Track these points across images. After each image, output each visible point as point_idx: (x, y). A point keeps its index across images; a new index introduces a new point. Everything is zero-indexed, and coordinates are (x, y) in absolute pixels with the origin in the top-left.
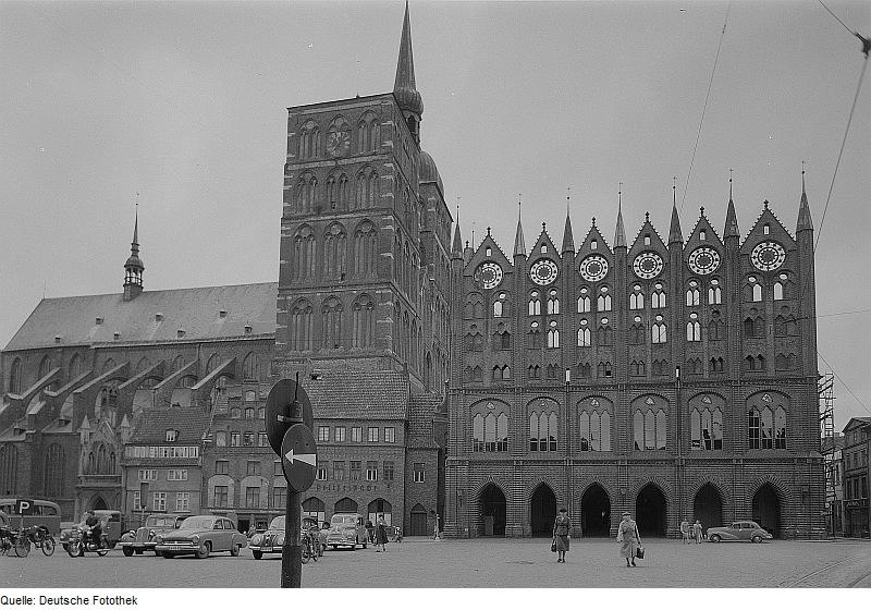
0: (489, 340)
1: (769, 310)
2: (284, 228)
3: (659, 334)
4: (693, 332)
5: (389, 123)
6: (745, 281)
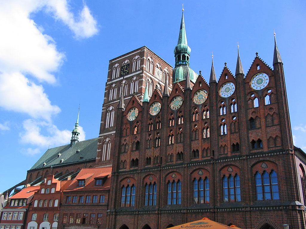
0: (130, 146)
1: (262, 111)
2: (103, 108)
3: (207, 134)
4: (224, 130)
5: (143, 58)
6: (248, 97)
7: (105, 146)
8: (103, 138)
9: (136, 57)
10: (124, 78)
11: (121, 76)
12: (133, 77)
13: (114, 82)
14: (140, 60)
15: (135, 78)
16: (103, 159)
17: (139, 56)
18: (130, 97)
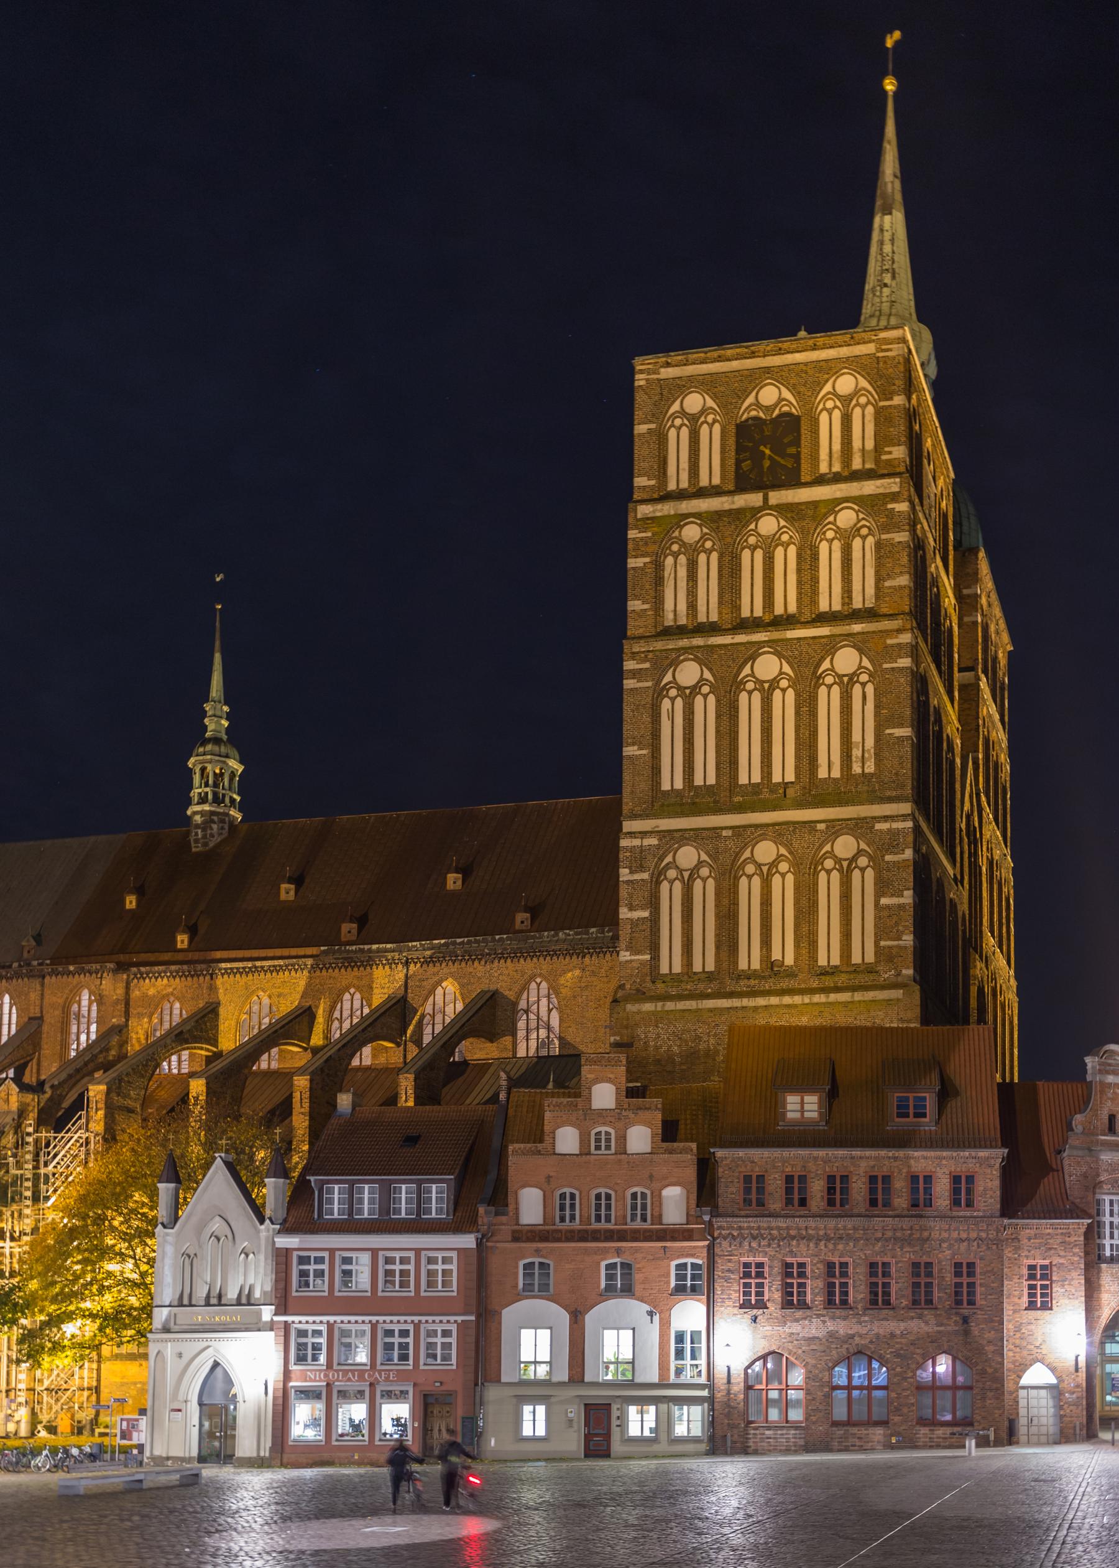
7: (671, 895)
8: (658, 847)
9: (846, 383)
10: (766, 499)
11: (743, 485)
12: (834, 505)
13: (697, 515)
14: (870, 410)
15: (846, 517)
16: (671, 961)
17: (864, 383)
18: (824, 631)
